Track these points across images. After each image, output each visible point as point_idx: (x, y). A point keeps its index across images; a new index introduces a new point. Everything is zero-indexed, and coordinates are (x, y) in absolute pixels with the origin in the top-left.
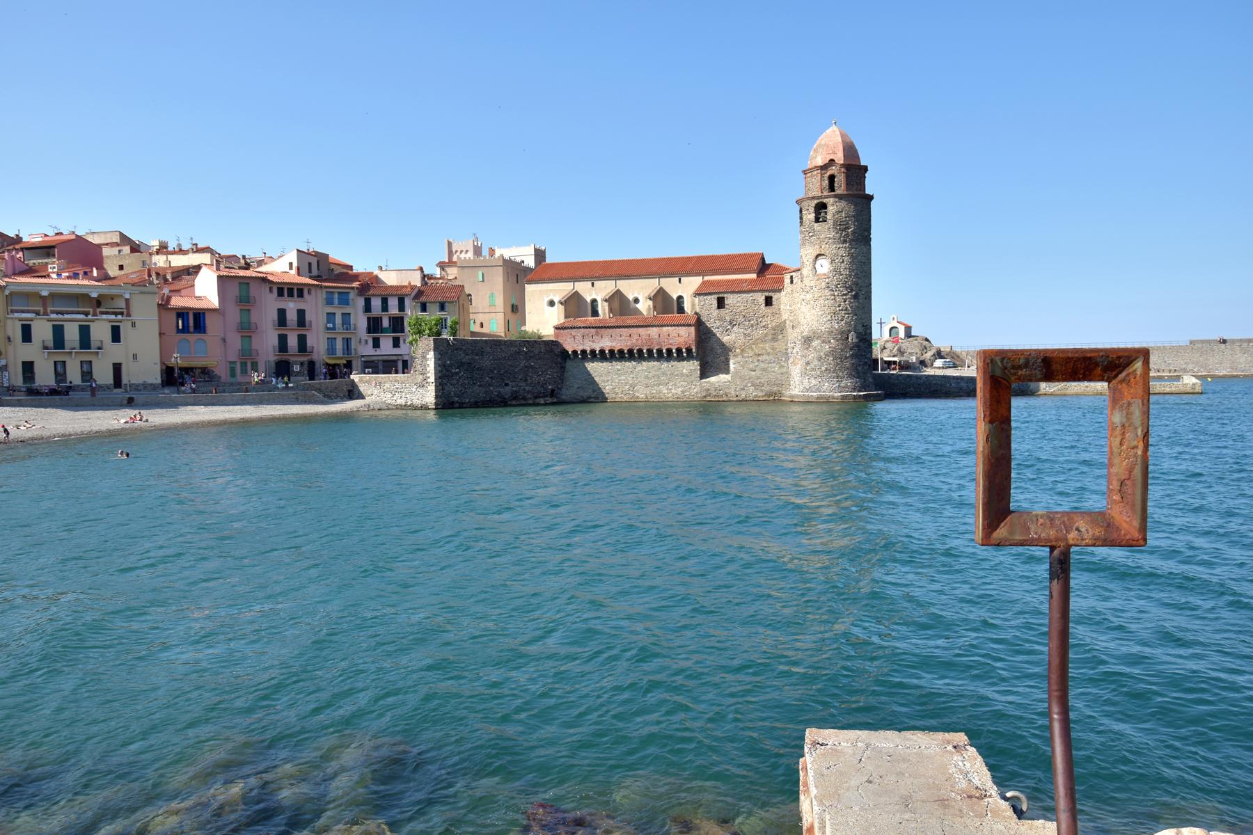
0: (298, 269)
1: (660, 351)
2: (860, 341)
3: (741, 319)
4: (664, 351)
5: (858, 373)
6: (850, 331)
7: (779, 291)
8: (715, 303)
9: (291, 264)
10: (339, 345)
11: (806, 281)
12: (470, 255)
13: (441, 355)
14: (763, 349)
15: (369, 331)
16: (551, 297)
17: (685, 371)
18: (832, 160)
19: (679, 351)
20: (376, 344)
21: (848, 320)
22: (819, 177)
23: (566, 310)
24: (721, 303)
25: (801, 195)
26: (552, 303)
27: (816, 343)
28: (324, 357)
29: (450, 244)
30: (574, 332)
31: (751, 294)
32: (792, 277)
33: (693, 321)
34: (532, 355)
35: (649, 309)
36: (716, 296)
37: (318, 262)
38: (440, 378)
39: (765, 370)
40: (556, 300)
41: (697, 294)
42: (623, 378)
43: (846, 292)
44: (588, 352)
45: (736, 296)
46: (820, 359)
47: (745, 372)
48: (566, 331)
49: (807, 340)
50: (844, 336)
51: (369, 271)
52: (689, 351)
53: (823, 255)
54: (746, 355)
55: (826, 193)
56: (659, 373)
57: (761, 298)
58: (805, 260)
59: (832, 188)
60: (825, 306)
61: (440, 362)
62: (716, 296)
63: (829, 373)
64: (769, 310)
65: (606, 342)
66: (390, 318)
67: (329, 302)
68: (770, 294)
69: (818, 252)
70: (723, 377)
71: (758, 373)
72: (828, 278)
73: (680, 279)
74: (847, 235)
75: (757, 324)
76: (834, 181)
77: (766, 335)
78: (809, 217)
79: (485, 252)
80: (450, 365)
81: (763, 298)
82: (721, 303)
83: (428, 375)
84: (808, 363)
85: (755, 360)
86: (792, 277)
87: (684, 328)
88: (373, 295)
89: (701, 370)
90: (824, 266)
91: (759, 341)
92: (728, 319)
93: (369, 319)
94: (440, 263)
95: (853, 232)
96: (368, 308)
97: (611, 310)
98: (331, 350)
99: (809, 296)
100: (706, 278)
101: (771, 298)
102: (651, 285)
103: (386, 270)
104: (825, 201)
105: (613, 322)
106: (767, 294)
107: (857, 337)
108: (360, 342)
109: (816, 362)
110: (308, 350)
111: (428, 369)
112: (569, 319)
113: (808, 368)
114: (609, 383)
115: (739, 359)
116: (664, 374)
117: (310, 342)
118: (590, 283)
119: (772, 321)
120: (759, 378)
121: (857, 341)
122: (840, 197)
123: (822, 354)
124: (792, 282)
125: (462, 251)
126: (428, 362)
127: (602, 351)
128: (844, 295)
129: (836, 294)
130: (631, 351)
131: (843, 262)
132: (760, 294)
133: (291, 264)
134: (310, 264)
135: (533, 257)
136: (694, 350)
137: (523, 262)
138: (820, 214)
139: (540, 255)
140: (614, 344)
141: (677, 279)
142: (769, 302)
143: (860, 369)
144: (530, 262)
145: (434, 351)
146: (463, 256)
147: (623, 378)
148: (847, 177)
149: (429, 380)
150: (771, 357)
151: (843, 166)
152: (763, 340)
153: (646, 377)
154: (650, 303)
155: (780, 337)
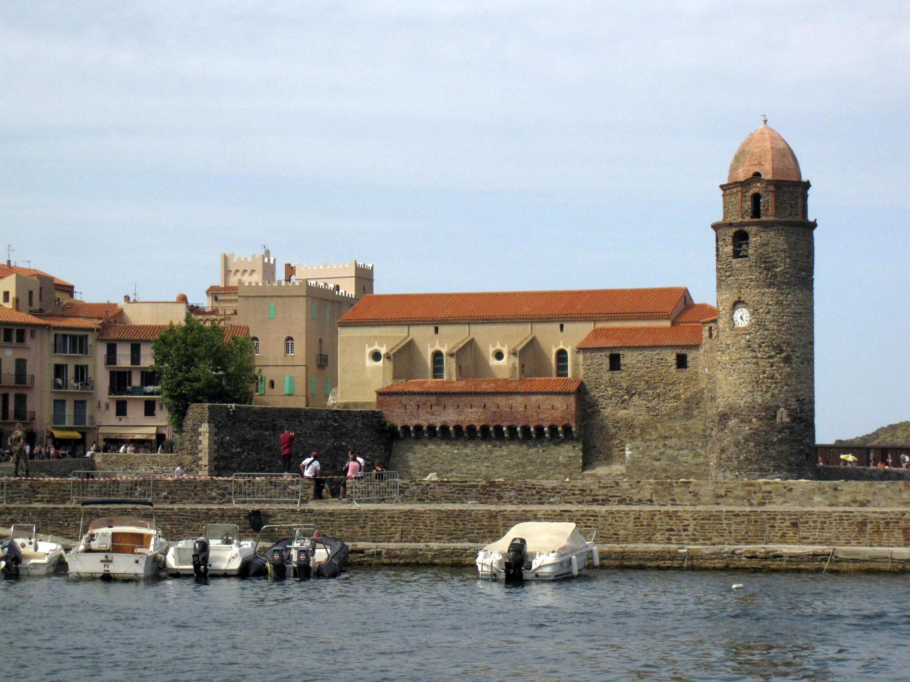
0: (17, 301)
1: (525, 429)
2: (793, 420)
3: (642, 386)
4: (532, 429)
5: (789, 464)
6: (778, 407)
7: (697, 347)
8: (607, 361)
9: (6, 294)
10: (69, 410)
11: (722, 337)
12: (256, 279)
13: (218, 429)
14: (671, 429)
15: (113, 390)
16: (376, 347)
17: (561, 459)
18: (757, 175)
19: (553, 429)
20: (121, 410)
21: (776, 392)
22: (740, 194)
23: (395, 367)
24: (615, 363)
25: (719, 218)
26: (376, 356)
27: (732, 422)
28: (49, 427)
29: (226, 259)
30: (404, 399)
31: (658, 352)
32: (710, 328)
33: (573, 387)
34: (344, 431)
35: (514, 368)
36: (608, 354)
37: (41, 289)
38: (216, 459)
39: (674, 459)
40: (383, 351)
41: (581, 350)
42: (474, 467)
43: (773, 353)
44: (425, 428)
45: (636, 353)
46: (737, 444)
47: (646, 462)
48: (394, 398)
49: (724, 417)
50: (769, 413)
51: (113, 301)
52: (567, 429)
53: (743, 302)
54: (647, 437)
55: (747, 219)
56: (524, 460)
57: (671, 357)
59: (756, 213)
61: (216, 438)
63: (750, 464)
64: (683, 374)
65: (449, 416)
66: (142, 373)
67: (57, 348)
68: (684, 352)
69: (736, 299)
70: (617, 468)
71: (663, 463)
72: (749, 334)
73: (562, 327)
74: (775, 276)
75: (665, 394)
76: (759, 203)
77: (676, 409)
78: (726, 249)
79: (280, 274)
80: (230, 444)
82: (615, 363)
83: (200, 455)
84: (723, 451)
85: (660, 445)
86: (710, 328)
87: (560, 398)
88: (121, 340)
89: (584, 457)
90: (742, 317)
91: (666, 418)
92: (624, 385)
93: (113, 374)
94: (212, 288)
95: (783, 273)
96: (111, 358)
97: (460, 368)
98: (58, 418)
99: (725, 358)
100: (599, 325)
102: (520, 334)
103: (135, 302)
104: (746, 229)
105: (461, 386)
106: (679, 351)
107: (789, 415)
108: (99, 406)
109: (732, 449)
110: (28, 416)
111: (200, 447)
112: (400, 381)
113: (723, 456)
114: (454, 474)
115: (638, 443)
116: (532, 462)
117: (30, 407)
118: (431, 329)
119: (686, 390)
120: (665, 470)
121: (788, 420)
122: (766, 226)
123: (740, 437)
124: (711, 336)
125: (245, 271)
126: (200, 438)
127: (445, 428)
128: (770, 357)
129: (759, 355)
130: (485, 429)
131: (768, 312)
132: (669, 351)
133: (6, 294)
134: (31, 293)
135: (353, 279)
136: (574, 429)
137: (337, 288)
138: (740, 246)
139: (364, 277)
140: (462, 418)
141: (558, 325)
142: (682, 362)
143: (793, 459)
144: (348, 289)
145: (209, 422)
146: (247, 279)
147: (474, 467)
148: (777, 198)
149: (200, 462)
150: (683, 440)
151: (768, 181)
152: (671, 417)
153: (507, 467)
154: (516, 361)
155: (696, 412)
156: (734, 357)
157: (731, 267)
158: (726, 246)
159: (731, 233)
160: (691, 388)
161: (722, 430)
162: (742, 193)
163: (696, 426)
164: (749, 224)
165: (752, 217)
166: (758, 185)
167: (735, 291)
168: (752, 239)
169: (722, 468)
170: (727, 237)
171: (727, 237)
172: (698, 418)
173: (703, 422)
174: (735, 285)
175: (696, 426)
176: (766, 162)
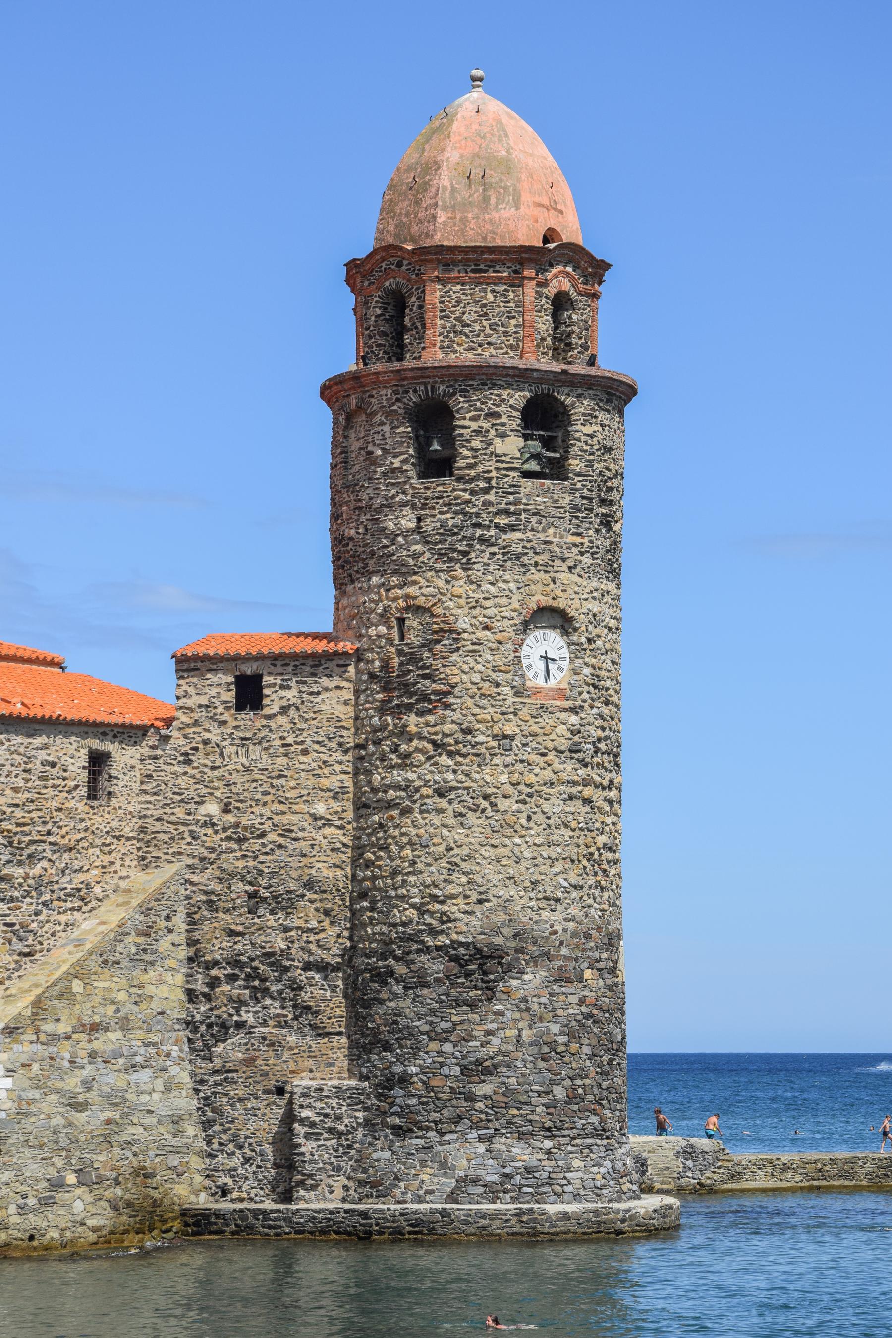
58: (463, 624)
60: (566, 825)
69: (546, 601)
123: (555, 1028)
155: (164, 945)
156: (532, 779)
157: (516, 503)
158: (503, 436)
159: (519, 397)
160: (117, 866)
161: (472, 1005)
162: (539, 285)
163: (163, 991)
165: (555, 357)
166: (569, 269)
169: (475, 1126)
170: (503, 409)
171: (503, 409)
172: (170, 963)
173: (180, 979)
174: (538, 558)
175: (163, 991)
176: (565, 205)
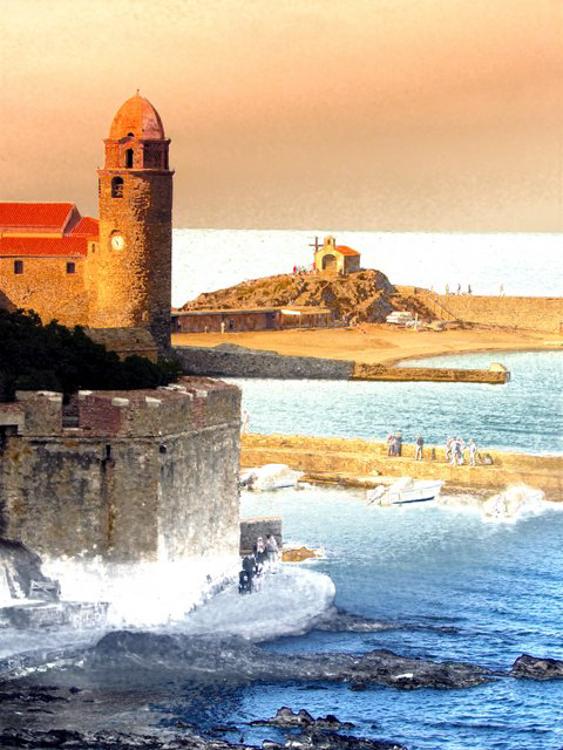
8: (13, 266)
36: (14, 260)
43: (140, 270)
57: (63, 266)
59: (130, 164)
62: (14, 260)
64: (71, 278)
81: (65, 264)
90: (119, 243)
101: (73, 265)
104: (122, 176)
122: (137, 175)
124: (94, 251)
131: (138, 239)
138: (117, 188)
142: (70, 268)
148: (145, 152)
164: (122, 173)
167: (114, 223)
168: (125, 184)
